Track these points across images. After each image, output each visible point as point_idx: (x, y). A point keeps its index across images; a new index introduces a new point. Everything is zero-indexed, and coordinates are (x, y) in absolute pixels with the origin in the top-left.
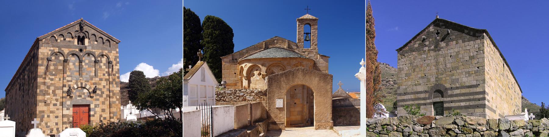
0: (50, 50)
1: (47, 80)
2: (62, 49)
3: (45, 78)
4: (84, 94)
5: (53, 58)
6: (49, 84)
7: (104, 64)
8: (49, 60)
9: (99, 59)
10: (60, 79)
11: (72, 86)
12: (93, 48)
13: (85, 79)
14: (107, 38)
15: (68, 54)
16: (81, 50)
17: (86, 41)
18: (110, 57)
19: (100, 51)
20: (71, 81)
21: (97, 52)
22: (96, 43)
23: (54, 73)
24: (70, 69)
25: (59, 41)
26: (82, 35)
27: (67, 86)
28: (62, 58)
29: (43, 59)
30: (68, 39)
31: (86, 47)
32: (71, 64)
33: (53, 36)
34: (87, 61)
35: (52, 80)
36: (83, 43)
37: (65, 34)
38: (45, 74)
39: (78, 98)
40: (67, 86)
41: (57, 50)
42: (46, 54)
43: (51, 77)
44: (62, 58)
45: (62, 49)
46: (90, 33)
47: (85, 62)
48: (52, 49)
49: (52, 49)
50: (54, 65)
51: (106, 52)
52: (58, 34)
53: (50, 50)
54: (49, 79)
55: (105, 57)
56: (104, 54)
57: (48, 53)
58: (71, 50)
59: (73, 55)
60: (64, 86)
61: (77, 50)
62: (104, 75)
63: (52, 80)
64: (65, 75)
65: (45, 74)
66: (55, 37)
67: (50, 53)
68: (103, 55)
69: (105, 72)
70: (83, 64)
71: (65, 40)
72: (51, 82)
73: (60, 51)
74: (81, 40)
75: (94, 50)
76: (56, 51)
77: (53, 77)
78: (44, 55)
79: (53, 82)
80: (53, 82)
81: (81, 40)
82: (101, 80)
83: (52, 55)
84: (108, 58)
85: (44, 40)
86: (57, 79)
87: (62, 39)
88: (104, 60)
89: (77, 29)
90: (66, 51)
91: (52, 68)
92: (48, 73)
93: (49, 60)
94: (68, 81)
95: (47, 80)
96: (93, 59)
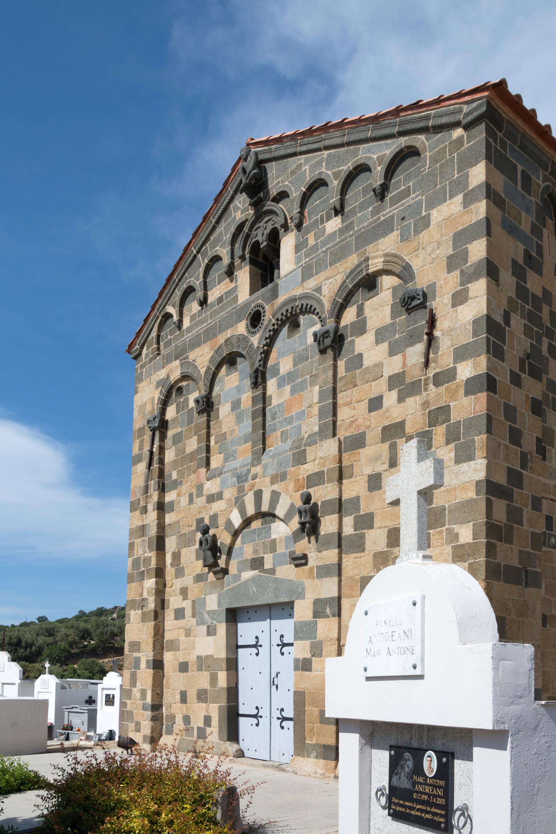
4: (272, 546)
7: (381, 335)
11: (221, 521)
13: (271, 471)
18: (416, 264)
20: (219, 496)
39: (248, 574)
41: (175, 370)
47: (276, 371)
58: (221, 339)
61: (242, 328)
62: (376, 404)
69: (380, 387)
82: (358, 442)
88: (379, 308)
94: (211, 499)
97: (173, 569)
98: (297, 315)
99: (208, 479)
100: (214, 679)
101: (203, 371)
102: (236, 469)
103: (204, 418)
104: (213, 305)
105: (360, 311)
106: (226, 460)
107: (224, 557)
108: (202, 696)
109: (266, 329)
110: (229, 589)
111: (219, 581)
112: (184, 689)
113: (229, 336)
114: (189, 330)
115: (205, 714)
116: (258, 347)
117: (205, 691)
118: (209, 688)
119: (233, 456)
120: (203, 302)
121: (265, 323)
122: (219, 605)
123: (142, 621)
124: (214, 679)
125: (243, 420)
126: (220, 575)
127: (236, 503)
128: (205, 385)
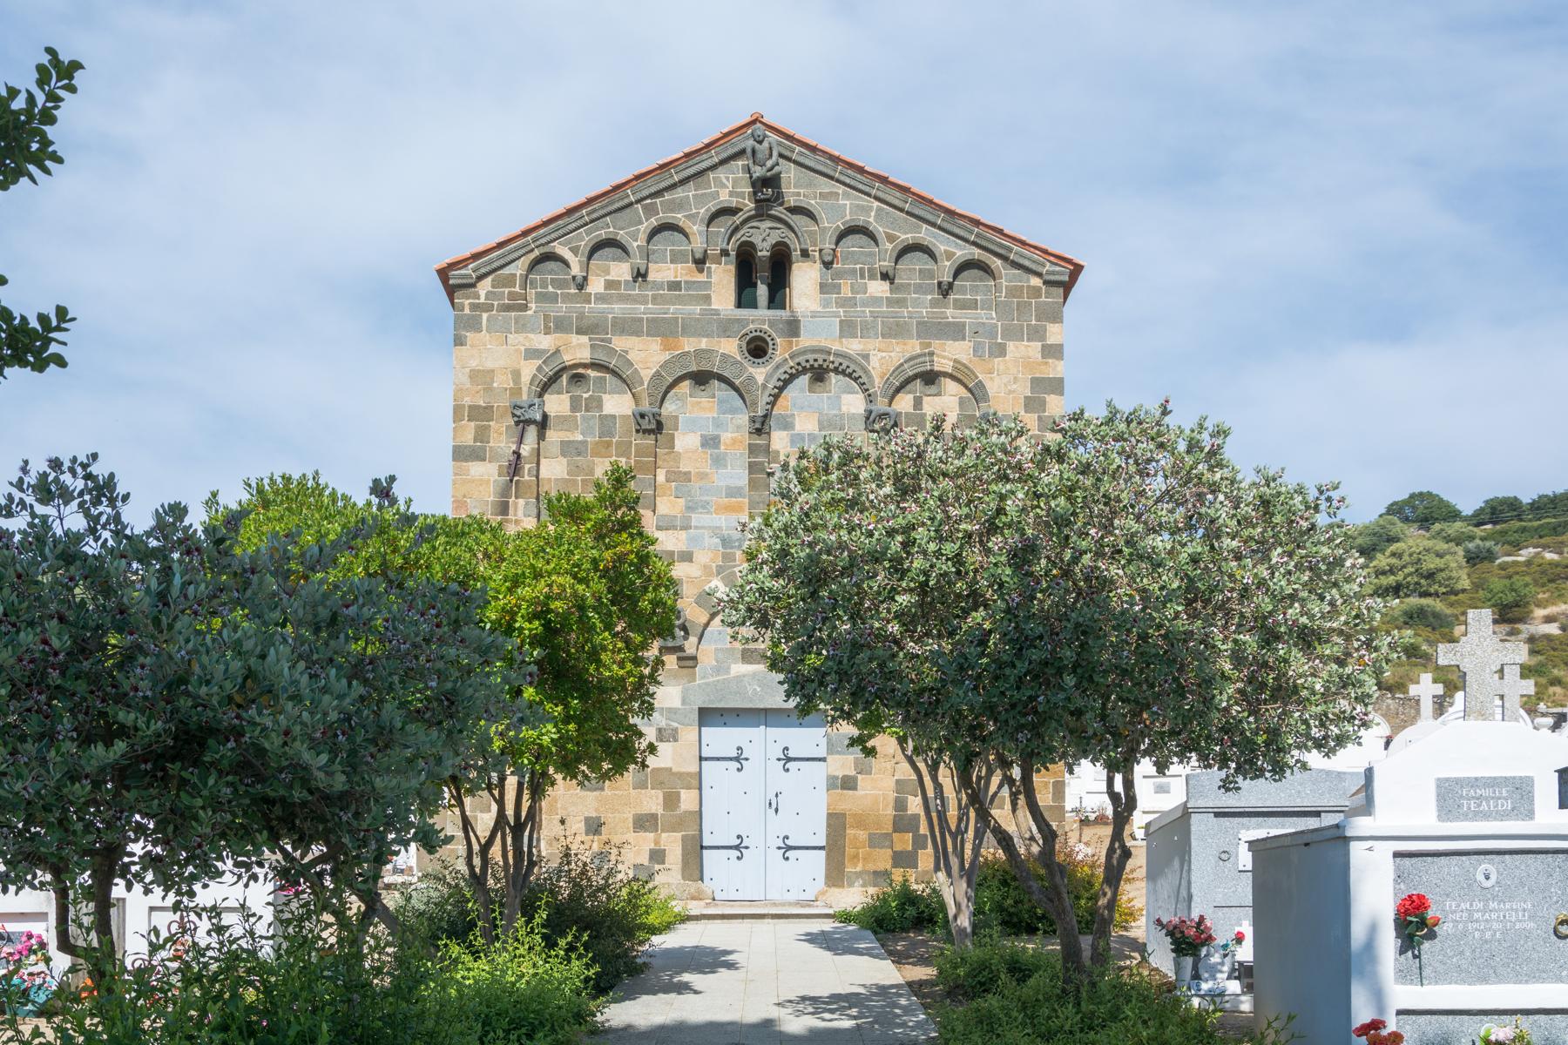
2: (619, 343)
12: (848, 329)
14: (963, 252)
15: (657, 375)
16: (758, 349)
17: (804, 279)
19: (914, 346)
21: (883, 358)
22: (878, 288)
25: (596, 286)
26: (764, 238)
28: (618, 404)
30: (662, 272)
31: (793, 328)
33: (550, 257)
37: (634, 233)
41: (578, 349)
44: (618, 404)
45: (619, 343)
48: (546, 342)
49: (546, 342)
51: (950, 353)
52: (586, 239)
53: (531, 354)
55: (950, 386)
56: (943, 364)
57: (516, 374)
58: (689, 345)
59: (701, 378)
61: (731, 347)
67: (528, 370)
68: (930, 378)
71: (640, 275)
73: (602, 357)
74: (760, 275)
75: (853, 346)
76: (568, 358)
78: (489, 389)
81: (760, 275)
83: (547, 386)
84: (977, 393)
85: (485, 287)
87: (621, 271)
89: (724, 198)
96: (854, 404)
98: (827, 370)
100: (671, 801)
101: (646, 375)
102: (720, 528)
103: (649, 441)
104: (658, 285)
105: (918, 403)
106: (689, 508)
107: (693, 640)
108: (644, 823)
109: (777, 367)
110: (707, 684)
111: (685, 671)
112: (594, 815)
113: (703, 346)
114: (600, 298)
115: (652, 846)
116: (764, 386)
117: (654, 817)
118: (660, 811)
119: (703, 507)
120: (640, 275)
121: (778, 359)
122: (684, 703)
124: (671, 801)
125: (725, 466)
126: (690, 663)
127: (719, 573)
128: (650, 395)
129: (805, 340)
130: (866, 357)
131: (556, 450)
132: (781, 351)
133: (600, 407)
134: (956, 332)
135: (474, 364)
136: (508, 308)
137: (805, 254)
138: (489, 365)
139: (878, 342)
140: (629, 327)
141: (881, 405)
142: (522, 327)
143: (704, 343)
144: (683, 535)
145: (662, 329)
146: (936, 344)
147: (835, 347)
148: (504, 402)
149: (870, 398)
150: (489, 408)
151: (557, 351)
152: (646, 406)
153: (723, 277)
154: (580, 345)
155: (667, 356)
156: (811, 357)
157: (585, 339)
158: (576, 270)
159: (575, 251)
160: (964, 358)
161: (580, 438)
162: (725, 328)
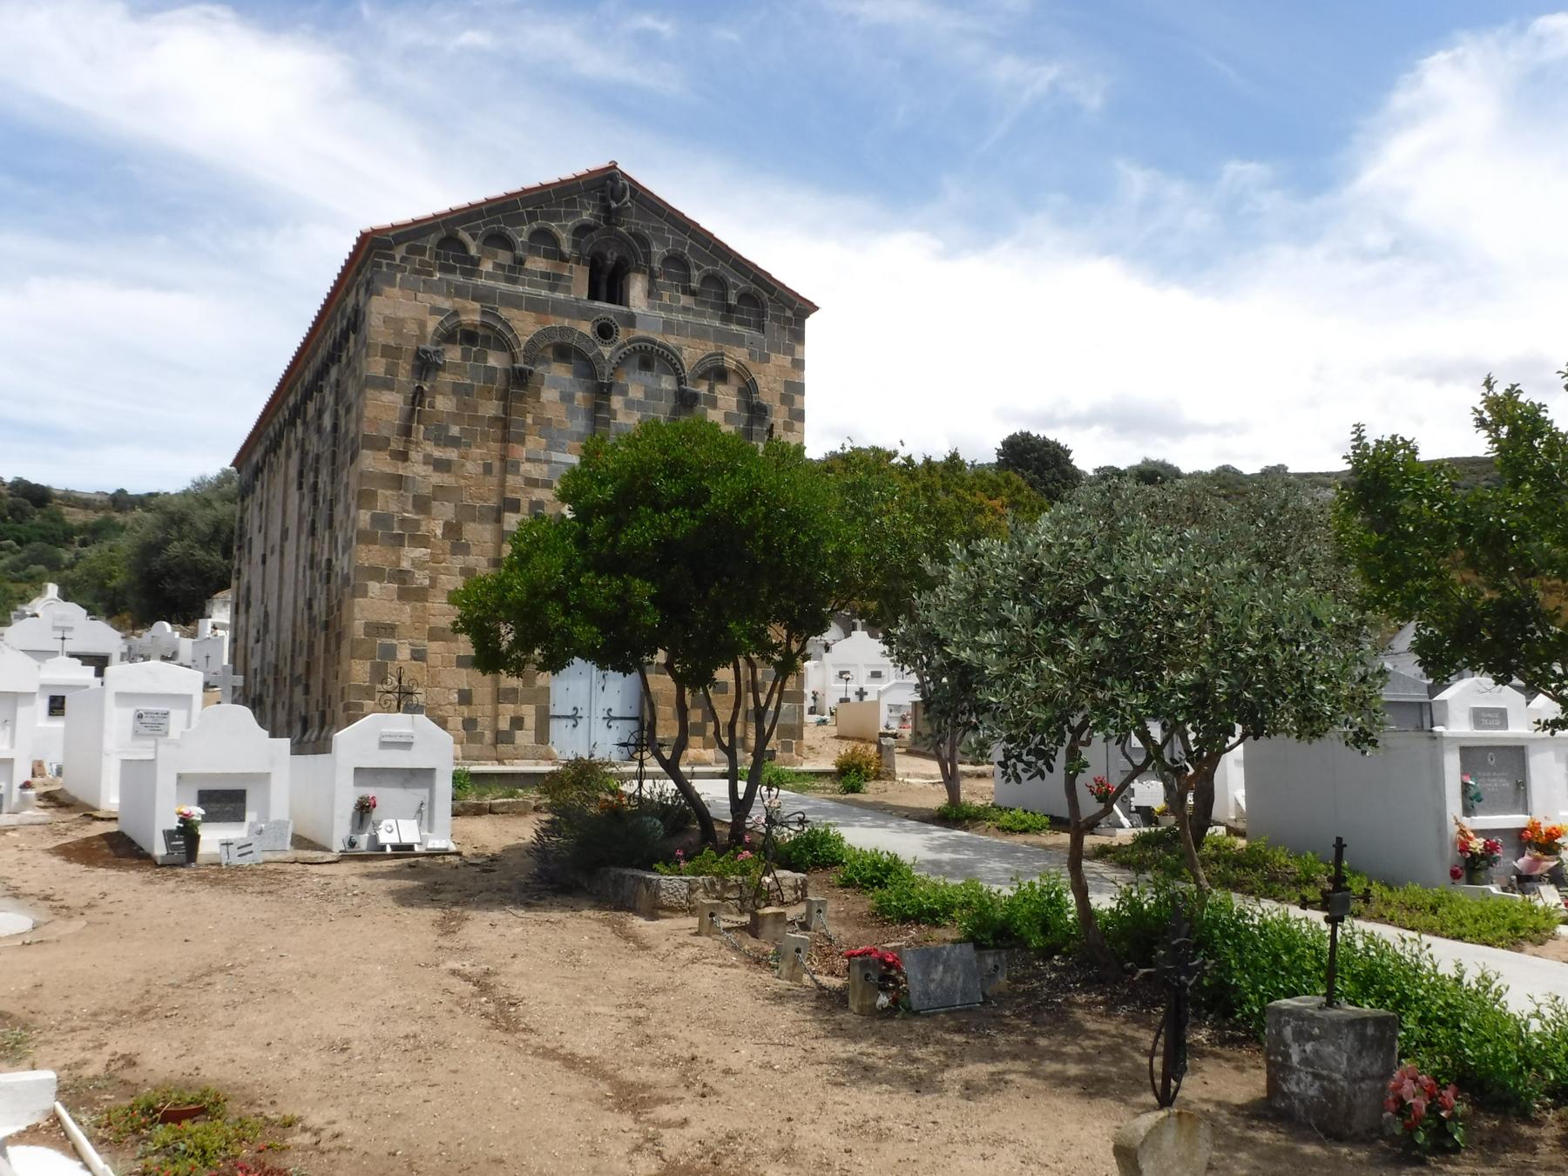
0: (435, 310)
1: (416, 468)
3: (403, 456)
5: (453, 354)
6: (426, 491)
8: (425, 365)
9: (703, 389)
10: (487, 469)
12: (668, 327)
16: (605, 331)
17: (637, 289)
18: (761, 383)
19: (711, 347)
23: (455, 430)
24: (544, 425)
25: (487, 266)
27: (525, 506)
29: (390, 352)
32: (549, 395)
34: (636, 393)
35: (442, 466)
36: (616, 294)
38: (406, 431)
40: (525, 506)
41: (472, 315)
42: (411, 328)
43: (438, 453)
45: (504, 313)
46: (658, 251)
47: (624, 392)
48: (446, 304)
49: (446, 304)
50: (457, 389)
51: (735, 356)
53: (435, 310)
54: (428, 460)
56: (730, 364)
57: (422, 325)
58: (556, 322)
59: (564, 353)
60: (514, 506)
61: (586, 328)
63: (442, 466)
64: (520, 452)
65: (406, 431)
66: (463, 247)
67: (432, 323)
70: (617, 402)
72: (437, 478)
75: (672, 341)
76: (464, 318)
77: (452, 454)
79: (446, 479)
80: (446, 479)
83: (448, 337)
84: (748, 388)
86: (472, 468)
90: (525, 326)
91: (444, 403)
92: (419, 431)
93: (425, 365)
94: (532, 483)
95: (416, 468)
96: (667, 384)
97: (448, 544)
99: (528, 460)
101: (524, 339)
105: (711, 389)
109: (619, 348)
123: (400, 598)
129: (639, 332)
130: (680, 350)
131: (448, 390)
132: (622, 336)
133: (485, 360)
134: (738, 340)
135: (387, 312)
136: (418, 272)
137: (638, 270)
138: (401, 315)
139: (688, 341)
140: (512, 301)
141: (689, 387)
142: (431, 288)
143: (567, 323)
144: (545, 467)
145: (534, 305)
146: (726, 348)
147: (659, 339)
148: (410, 347)
149: (680, 381)
150: (399, 348)
151: (456, 313)
152: (520, 365)
153: (580, 278)
154: (473, 311)
155: (539, 328)
156: (643, 344)
157: (477, 305)
158: (473, 251)
159: (474, 237)
160: (742, 360)
161: (468, 382)
162: (583, 314)
